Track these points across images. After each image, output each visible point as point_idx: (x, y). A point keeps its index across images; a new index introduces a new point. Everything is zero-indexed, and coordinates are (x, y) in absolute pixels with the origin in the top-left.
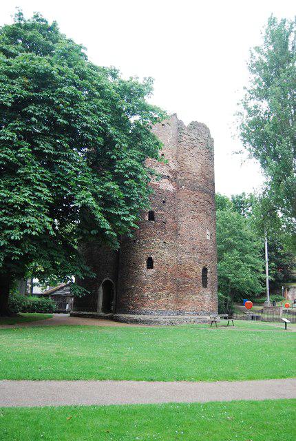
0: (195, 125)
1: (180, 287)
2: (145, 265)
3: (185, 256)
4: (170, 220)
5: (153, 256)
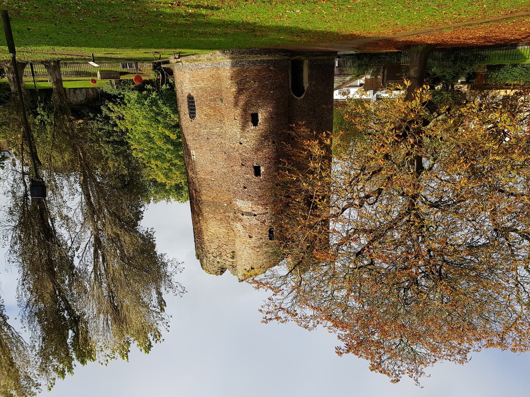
1: (217, 95)
2: (260, 117)
4: (237, 168)
5: (253, 127)
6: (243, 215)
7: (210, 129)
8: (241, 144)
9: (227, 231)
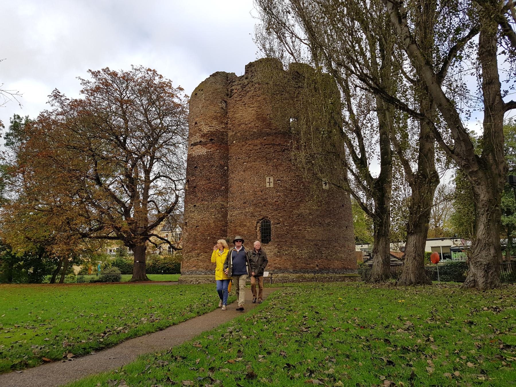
0: (249, 67)
3: (236, 212)
6: (200, 142)
7: (242, 213)
8: (195, 206)
9: (235, 116)
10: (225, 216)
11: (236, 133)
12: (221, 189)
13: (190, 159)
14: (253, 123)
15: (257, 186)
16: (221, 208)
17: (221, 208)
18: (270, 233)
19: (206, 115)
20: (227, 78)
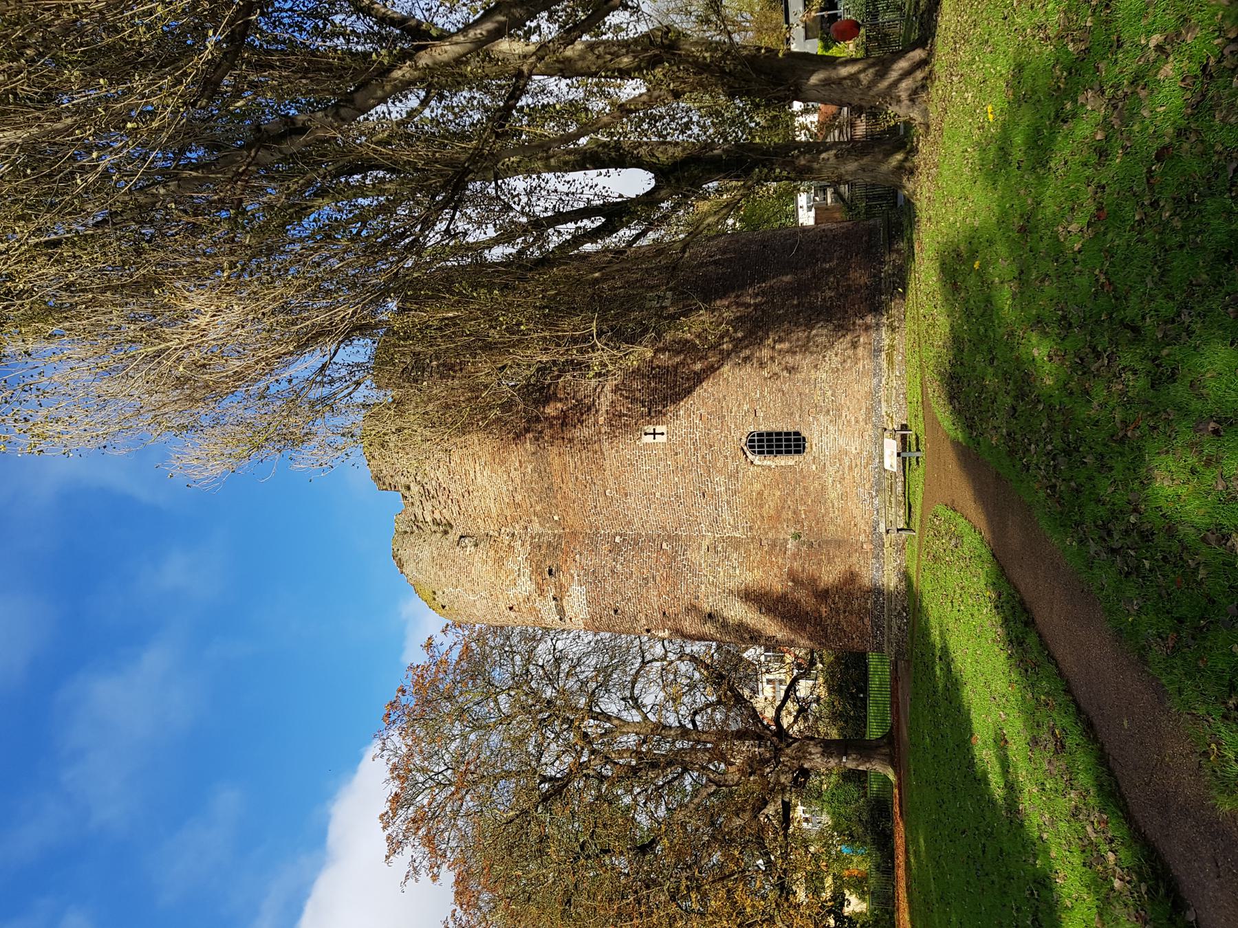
3: (726, 515)
7: (728, 502)
9: (494, 515)
10: (736, 544)
11: (535, 514)
12: (670, 552)
13: (597, 624)
14: (514, 474)
15: (662, 464)
16: (717, 552)
17: (717, 552)
18: (779, 434)
19: (493, 586)
20: (406, 532)
